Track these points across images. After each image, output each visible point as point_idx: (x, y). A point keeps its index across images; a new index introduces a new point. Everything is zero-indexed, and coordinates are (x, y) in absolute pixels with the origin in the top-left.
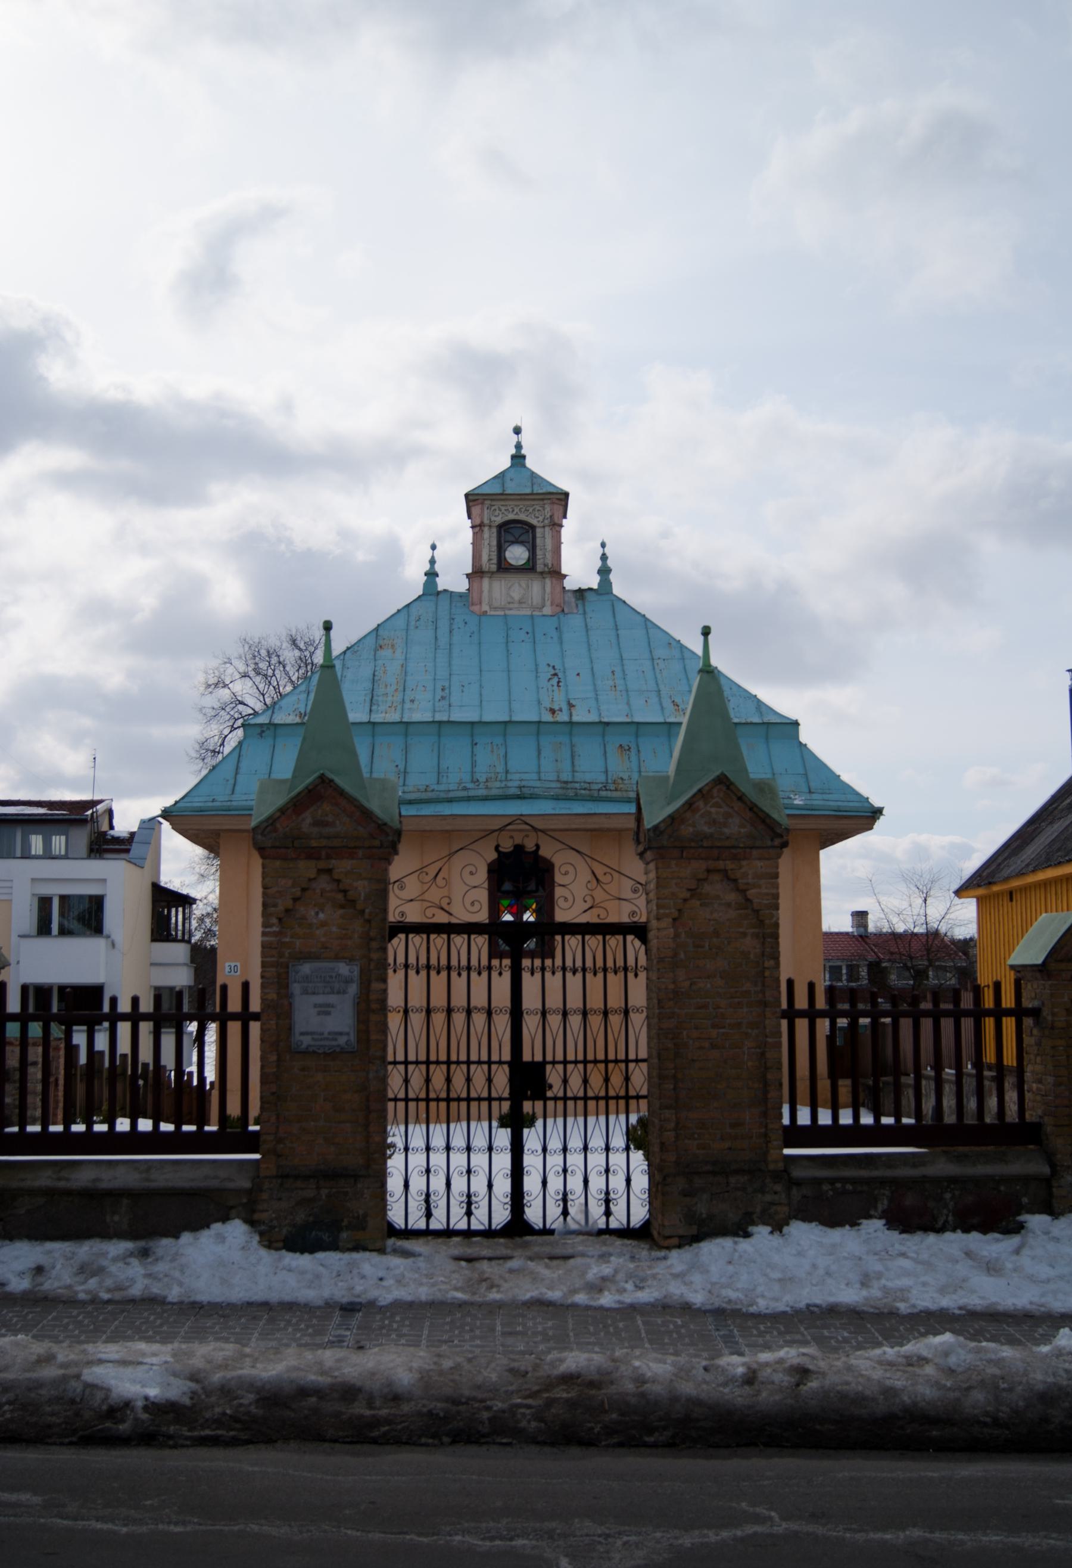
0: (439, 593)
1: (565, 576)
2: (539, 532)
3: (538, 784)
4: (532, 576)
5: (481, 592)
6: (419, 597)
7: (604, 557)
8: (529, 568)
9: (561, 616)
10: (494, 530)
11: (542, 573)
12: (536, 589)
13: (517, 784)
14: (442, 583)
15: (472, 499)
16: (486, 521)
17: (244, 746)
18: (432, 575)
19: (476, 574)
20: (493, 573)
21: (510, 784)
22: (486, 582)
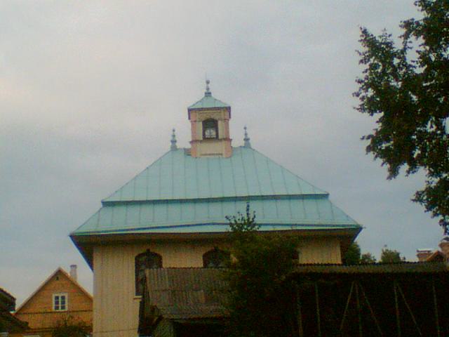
8: (217, 138)
10: (201, 123)
11: (221, 140)
14: (178, 145)
15: (190, 111)
18: (174, 142)
19: (193, 142)
20: (201, 141)
22: (198, 145)
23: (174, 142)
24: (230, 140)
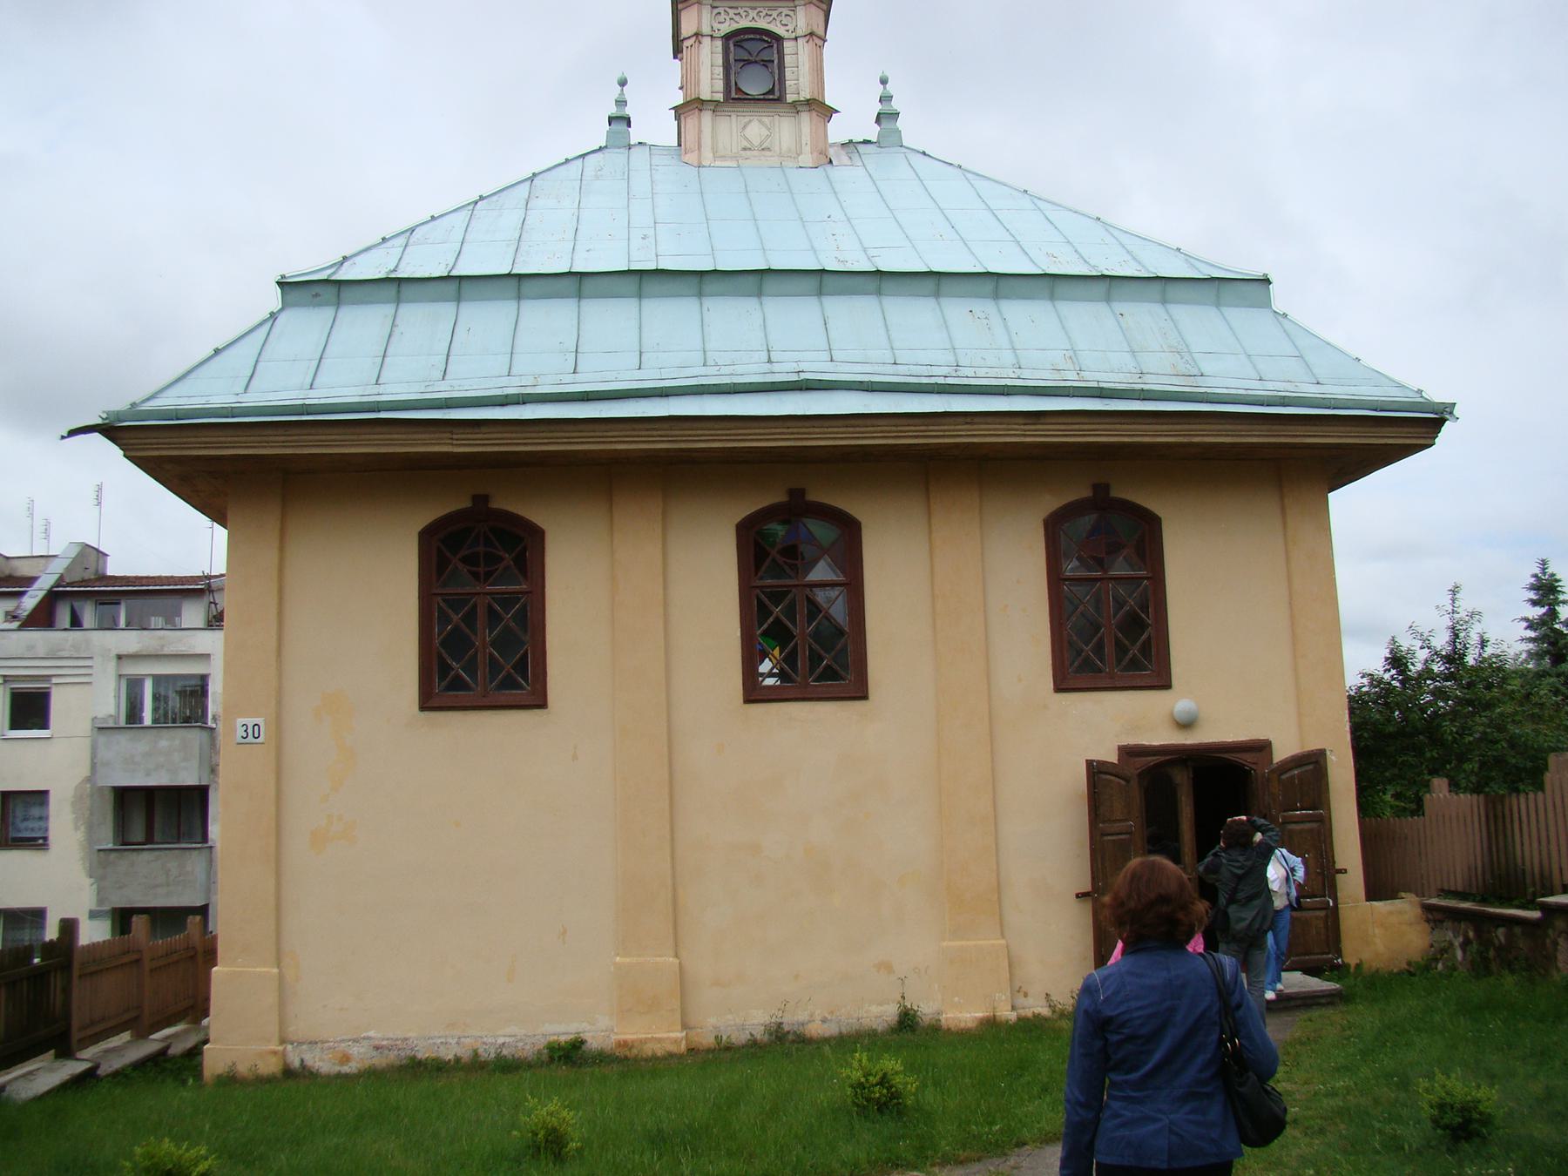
0: (630, 147)
1: (828, 112)
2: (788, 46)
3: (829, 366)
4: (779, 107)
5: (700, 131)
6: (601, 149)
7: (885, 99)
8: (774, 97)
9: (829, 167)
10: (719, 43)
11: (794, 104)
12: (785, 130)
13: (793, 367)
16: (706, 30)
17: (282, 319)
18: (620, 120)
21: (776, 367)
22: (707, 117)
23: (620, 120)
24: (828, 112)
